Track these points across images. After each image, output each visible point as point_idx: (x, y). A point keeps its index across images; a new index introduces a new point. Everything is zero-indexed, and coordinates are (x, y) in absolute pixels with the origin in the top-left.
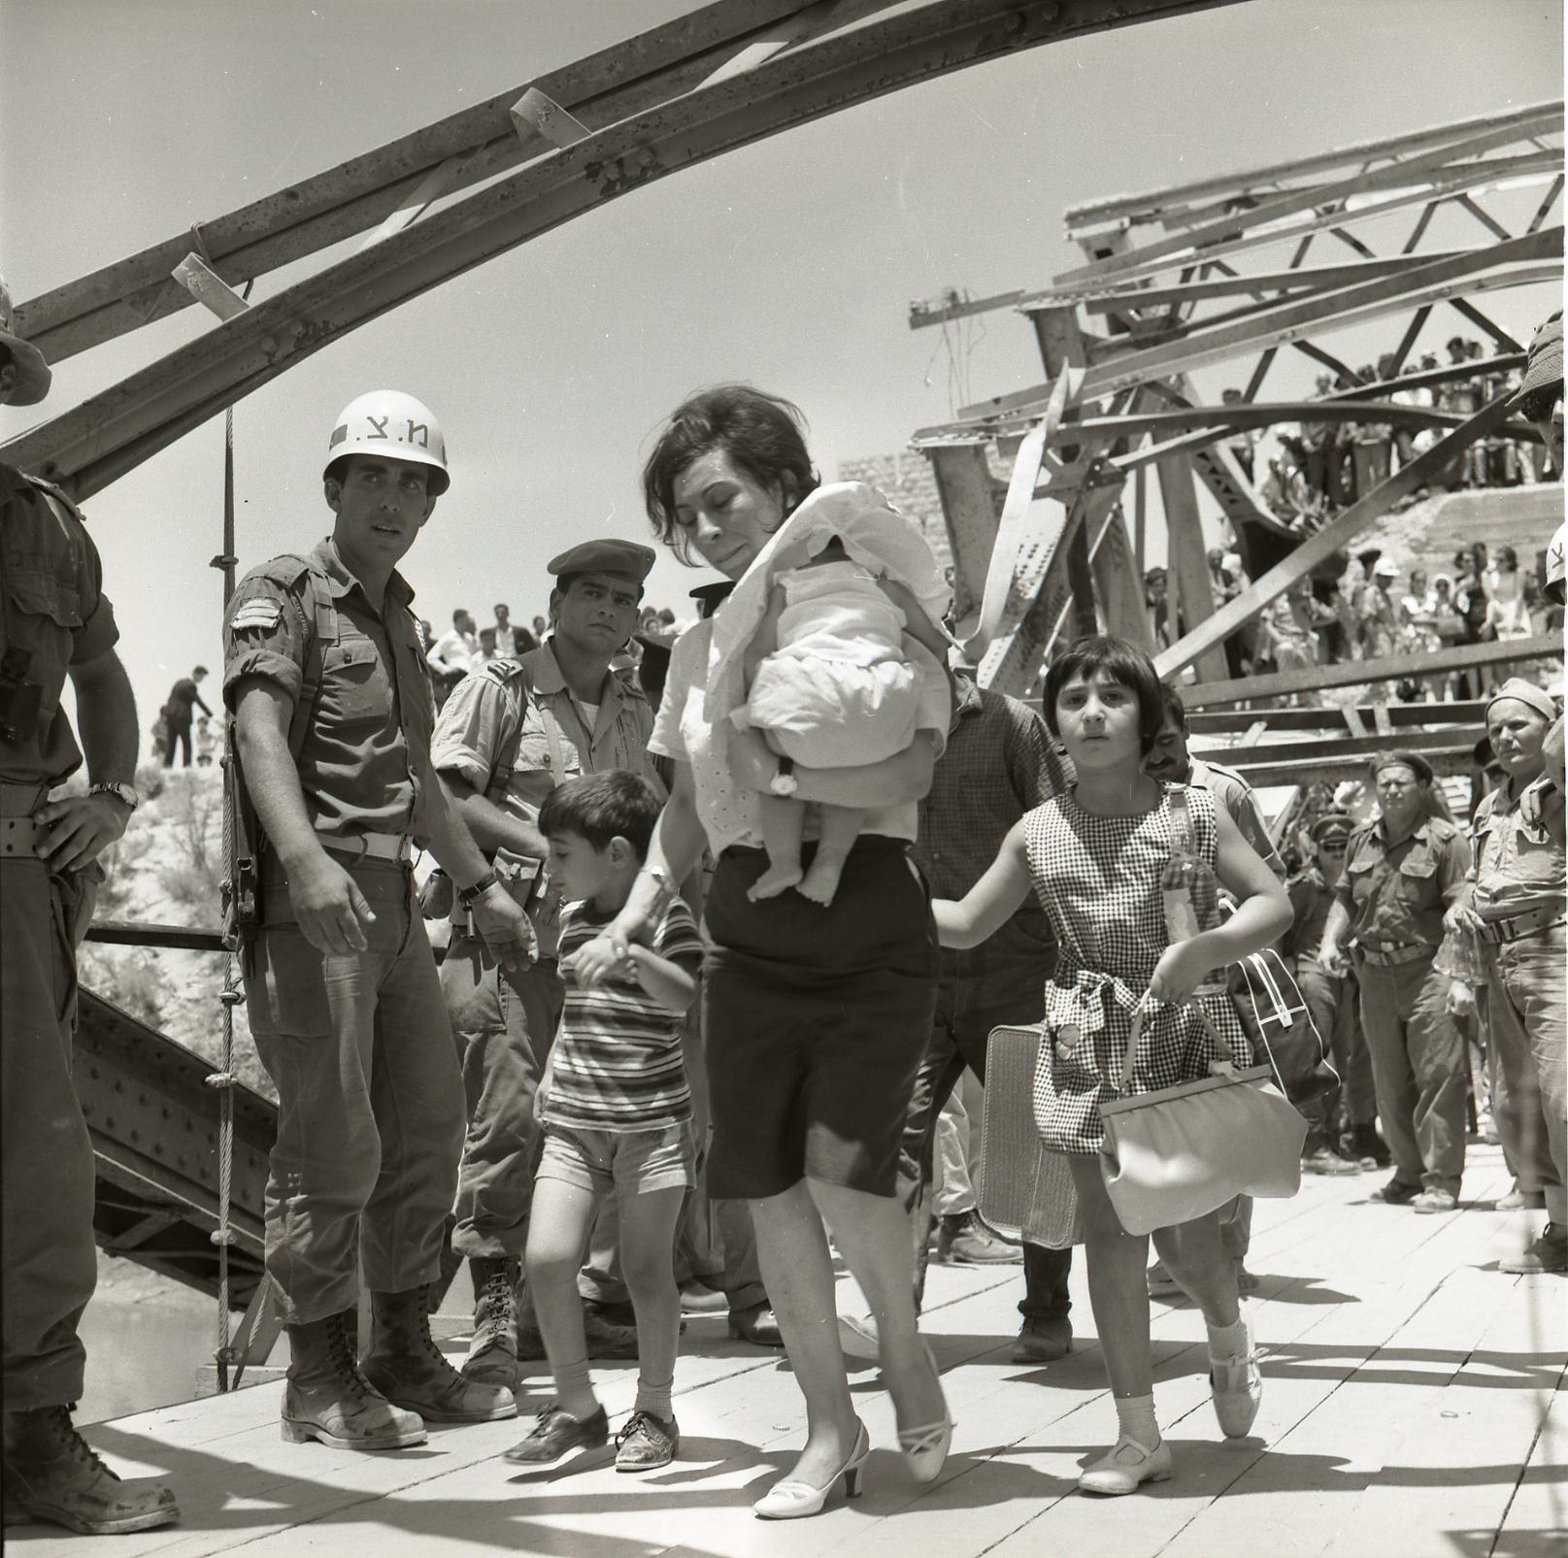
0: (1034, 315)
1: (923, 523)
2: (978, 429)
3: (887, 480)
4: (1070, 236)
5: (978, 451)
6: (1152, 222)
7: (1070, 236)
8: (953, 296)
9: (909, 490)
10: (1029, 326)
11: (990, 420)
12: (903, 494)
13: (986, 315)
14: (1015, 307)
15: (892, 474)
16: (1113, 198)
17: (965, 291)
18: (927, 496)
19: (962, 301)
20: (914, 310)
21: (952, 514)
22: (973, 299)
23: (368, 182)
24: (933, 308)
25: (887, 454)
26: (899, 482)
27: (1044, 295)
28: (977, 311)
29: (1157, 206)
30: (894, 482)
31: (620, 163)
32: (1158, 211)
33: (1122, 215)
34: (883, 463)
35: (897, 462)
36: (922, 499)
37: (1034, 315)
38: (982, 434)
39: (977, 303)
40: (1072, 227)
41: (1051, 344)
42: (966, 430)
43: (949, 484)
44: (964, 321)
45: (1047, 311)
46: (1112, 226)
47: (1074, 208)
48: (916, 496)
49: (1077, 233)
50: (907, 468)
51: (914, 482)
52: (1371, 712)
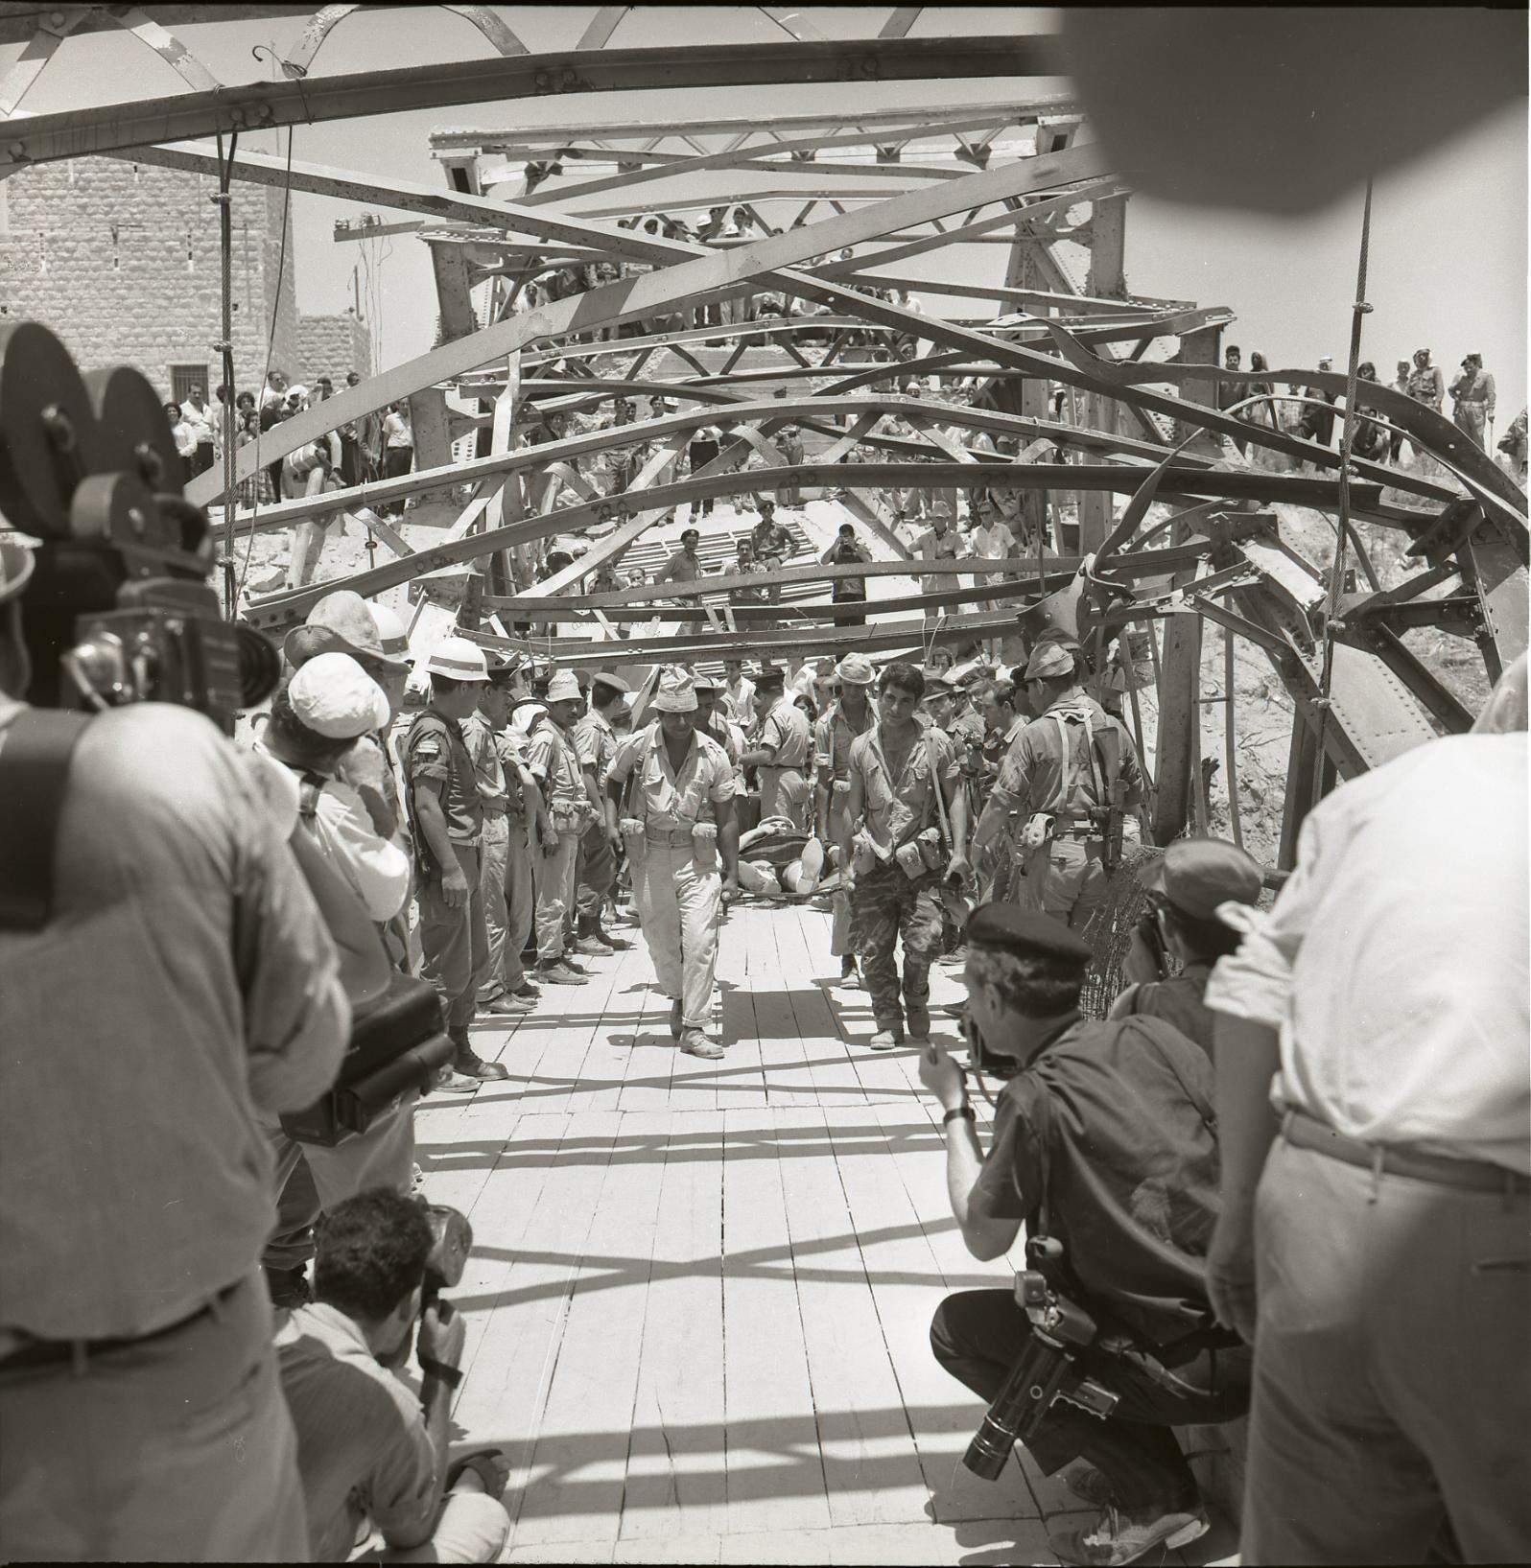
0: (432, 243)
1: (115, 236)
3: (59, 176)
4: (434, 155)
7: (434, 155)
8: (370, 220)
9: (83, 189)
10: (428, 250)
12: (76, 192)
14: (418, 234)
16: (470, 130)
18: (102, 198)
19: (376, 223)
20: (337, 226)
21: (417, 430)
22: (384, 223)
24: (353, 226)
26: (72, 180)
30: (67, 181)
31: (608, 506)
32: (505, 147)
36: (97, 200)
37: (432, 243)
39: (388, 227)
40: (435, 147)
41: (442, 265)
43: (416, 409)
44: (378, 239)
45: (441, 242)
46: (469, 152)
47: (438, 133)
49: (440, 153)
50: (80, 167)
51: (89, 181)
52: (723, 610)
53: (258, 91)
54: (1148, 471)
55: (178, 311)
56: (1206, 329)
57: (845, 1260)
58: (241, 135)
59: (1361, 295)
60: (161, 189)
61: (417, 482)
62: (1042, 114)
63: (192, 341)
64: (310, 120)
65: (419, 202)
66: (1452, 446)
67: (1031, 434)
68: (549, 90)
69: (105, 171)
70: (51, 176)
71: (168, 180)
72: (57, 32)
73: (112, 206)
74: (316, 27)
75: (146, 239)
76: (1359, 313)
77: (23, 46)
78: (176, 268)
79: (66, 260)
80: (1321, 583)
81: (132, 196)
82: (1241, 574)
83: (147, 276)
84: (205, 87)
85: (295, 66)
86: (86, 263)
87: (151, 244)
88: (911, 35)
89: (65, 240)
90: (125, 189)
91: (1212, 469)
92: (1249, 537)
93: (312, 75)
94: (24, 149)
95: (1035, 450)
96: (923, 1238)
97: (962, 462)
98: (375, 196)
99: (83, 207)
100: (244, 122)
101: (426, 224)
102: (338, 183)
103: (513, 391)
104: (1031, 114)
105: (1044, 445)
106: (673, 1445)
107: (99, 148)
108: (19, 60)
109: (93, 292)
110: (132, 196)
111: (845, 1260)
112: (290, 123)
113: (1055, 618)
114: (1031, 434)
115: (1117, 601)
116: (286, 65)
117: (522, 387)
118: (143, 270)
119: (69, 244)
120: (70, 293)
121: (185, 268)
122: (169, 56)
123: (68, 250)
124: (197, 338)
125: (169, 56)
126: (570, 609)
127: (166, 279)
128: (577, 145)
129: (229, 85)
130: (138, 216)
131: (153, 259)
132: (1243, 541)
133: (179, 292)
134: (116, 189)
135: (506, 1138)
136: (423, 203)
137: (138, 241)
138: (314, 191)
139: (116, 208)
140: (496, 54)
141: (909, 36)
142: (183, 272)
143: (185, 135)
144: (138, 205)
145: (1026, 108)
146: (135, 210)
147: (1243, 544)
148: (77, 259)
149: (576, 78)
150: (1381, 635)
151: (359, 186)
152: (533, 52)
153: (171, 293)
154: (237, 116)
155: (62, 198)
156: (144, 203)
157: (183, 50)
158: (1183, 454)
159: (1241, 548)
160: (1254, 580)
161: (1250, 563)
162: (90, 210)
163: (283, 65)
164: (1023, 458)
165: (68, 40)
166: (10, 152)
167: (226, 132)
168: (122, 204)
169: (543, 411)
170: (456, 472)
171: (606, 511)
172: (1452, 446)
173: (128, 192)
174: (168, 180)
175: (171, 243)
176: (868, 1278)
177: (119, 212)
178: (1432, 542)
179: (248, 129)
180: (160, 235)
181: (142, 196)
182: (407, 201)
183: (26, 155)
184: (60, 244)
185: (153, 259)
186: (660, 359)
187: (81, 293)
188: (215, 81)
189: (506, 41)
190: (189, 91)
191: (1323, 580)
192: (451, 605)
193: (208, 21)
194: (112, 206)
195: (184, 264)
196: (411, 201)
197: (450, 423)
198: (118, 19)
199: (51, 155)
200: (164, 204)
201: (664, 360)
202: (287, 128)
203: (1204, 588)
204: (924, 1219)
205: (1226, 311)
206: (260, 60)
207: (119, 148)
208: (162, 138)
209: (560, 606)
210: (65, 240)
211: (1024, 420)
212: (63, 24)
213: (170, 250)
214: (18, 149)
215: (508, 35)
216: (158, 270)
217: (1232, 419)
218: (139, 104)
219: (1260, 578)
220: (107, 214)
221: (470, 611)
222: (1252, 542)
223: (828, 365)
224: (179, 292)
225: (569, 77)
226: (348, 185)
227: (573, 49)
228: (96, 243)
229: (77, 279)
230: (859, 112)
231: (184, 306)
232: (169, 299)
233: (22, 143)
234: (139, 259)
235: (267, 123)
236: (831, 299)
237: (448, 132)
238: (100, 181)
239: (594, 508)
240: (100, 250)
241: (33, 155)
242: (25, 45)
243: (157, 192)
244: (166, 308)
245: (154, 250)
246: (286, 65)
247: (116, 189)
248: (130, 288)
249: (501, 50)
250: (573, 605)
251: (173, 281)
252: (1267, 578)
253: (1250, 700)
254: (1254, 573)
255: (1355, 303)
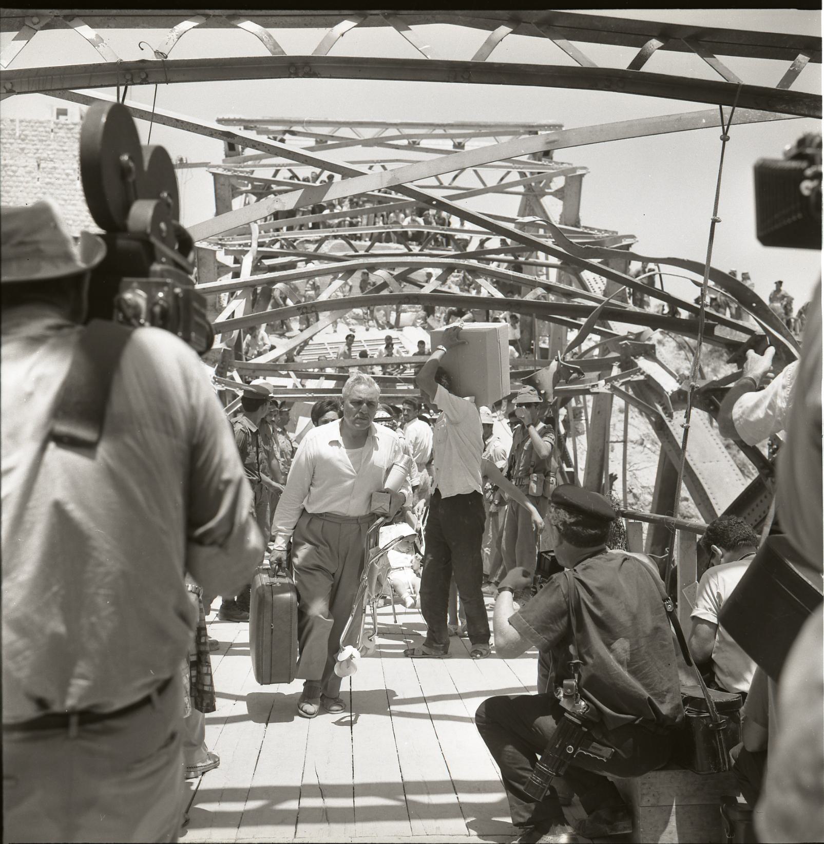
0: (214, 174)
1: (39, 165)
2: (218, 244)
3: (10, 132)
5: (214, 252)
6: (252, 130)
8: (181, 160)
9: (23, 140)
10: (212, 178)
11: (220, 240)
12: (19, 141)
13: (194, 169)
15: (13, 130)
16: (237, 117)
17: (186, 158)
18: (33, 145)
19: (185, 162)
23: (225, 287)
25: (12, 118)
26: (17, 135)
27: (219, 166)
28: (190, 167)
29: (255, 124)
30: (15, 134)
31: (306, 308)
32: (256, 127)
33: (240, 125)
34: (10, 122)
35: (17, 123)
37: (214, 174)
38: (219, 246)
39: (191, 164)
41: (218, 186)
42: (212, 243)
43: (201, 260)
44: (185, 170)
47: (221, 117)
48: (27, 144)
50: (22, 128)
51: (26, 136)
53: (141, 64)
54: (593, 308)
55: (70, 207)
56: (622, 246)
57: (420, 708)
58: (129, 87)
59: (715, 213)
60: (65, 143)
61: (204, 289)
62: (541, 130)
63: (76, 224)
64: (167, 82)
65: (220, 134)
66: (754, 305)
67: (533, 285)
68: (296, 75)
69: (36, 131)
70: (6, 132)
71: (69, 138)
72: (34, 27)
73: (38, 150)
74: (174, 34)
75: (55, 168)
76: (714, 222)
77: (15, 33)
78: (70, 184)
79: (11, 176)
80: (678, 381)
81: (49, 145)
82: (635, 374)
83: (54, 187)
84: (113, 60)
85: (162, 53)
86: (22, 179)
87: (57, 171)
88: (489, 60)
89: (11, 166)
90: (46, 141)
91: (627, 309)
92: (640, 355)
93: (170, 58)
94: (12, 86)
95: (535, 293)
96: (460, 700)
97: (496, 297)
98: (197, 129)
99: (23, 149)
100: (132, 80)
101: (212, 164)
102: (177, 120)
103: (253, 253)
104: (536, 129)
105: (540, 291)
106: (325, 792)
107: (53, 88)
108: (13, 40)
109: (25, 194)
110: (49, 145)
111: (420, 708)
112: (156, 83)
113: (541, 382)
114: (533, 285)
115: (575, 375)
116: (157, 52)
117: (258, 252)
118: (52, 184)
119: (14, 168)
120: (12, 194)
121: (75, 185)
122: (94, 43)
123: (13, 171)
124: (78, 222)
125: (94, 43)
126: (277, 371)
127: (65, 190)
128: (294, 129)
129: (125, 60)
130: (52, 156)
131: (58, 179)
132: (637, 357)
133: (71, 197)
134: (41, 141)
135: (232, 641)
136: (221, 135)
137: (51, 169)
138: (164, 124)
139: (40, 151)
140: (270, 54)
141: (486, 61)
142: (74, 187)
143: (100, 85)
144: (52, 150)
145: (533, 126)
146: (49, 153)
147: (637, 359)
148: (17, 176)
149: (310, 70)
150: (712, 403)
151: (188, 123)
152: (288, 54)
153: (66, 197)
154: (128, 77)
155: (11, 144)
156: (55, 149)
157: (102, 40)
158: (612, 301)
159: (636, 361)
160: (642, 377)
161: (640, 369)
162: (26, 151)
163: (155, 52)
164: (530, 297)
165: (40, 33)
166: (5, 87)
167: (122, 85)
168: (43, 149)
169: (269, 265)
170: (225, 285)
171: (305, 311)
172: (754, 305)
173: (48, 143)
174: (69, 138)
175: (67, 171)
176: (431, 717)
177: (41, 153)
178: (740, 356)
179: (134, 84)
180: (63, 166)
181: (54, 145)
182: (213, 133)
183: (14, 89)
184: (9, 168)
185: (58, 179)
186: (330, 246)
187: (19, 194)
188: (118, 58)
189: (275, 48)
190: (102, 61)
191: (679, 380)
192: (212, 364)
193: (115, 28)
194: (38, 150)
195: (74, 183)
196: (215, 133)
197: (218, 268)
198: (68, 23)
199: (27, 90)
200: (66, 151)
201: (332, 247)
202: (154, 86)
203: (616, 380)
204: (461, 692)
205: (633, 237)
206: (142, 49)
207: (63, 89)
208: (87, 85)
209: (271, 368)
210: (11, 166)
211: (530, 277)
212: (38, 23)
213: (68, 175)
214: (9, 86)
215: (276, 45)
216: (60, 185)
217: (639, 282)
218: (76, 66)
219: (646, 376)
220: (35, 153)
221: (222, 368)
222: (641, 358)
223: (423, 251)
224: (71, 197)
225: (307, 69)
226: (183, 122)
227: (310, 54)
228: (28, 169)
229: (17, 187)
230: (445, 122)
231: (74, 205)
232: (65, 200)
233: (11, 83)
234: (50, 178)
235: (145, 81)
236: (434, 203)
237: (226, 117)
238: (33, 136)
239: (299, 308)
240: (30, 172)
241: (17, 90)
242: (16, 33)
243: (62, 144)
244: (63, 205)
245: (59, 174)
246: (157, 52)
247: (41, 141)
248: (44, 193)
249: (273, 53)
250: (278, 368)
251: (68, 191)
252: (648, 377)
253: (634, 446)
254: (642, 374)
255: (712, 217)
